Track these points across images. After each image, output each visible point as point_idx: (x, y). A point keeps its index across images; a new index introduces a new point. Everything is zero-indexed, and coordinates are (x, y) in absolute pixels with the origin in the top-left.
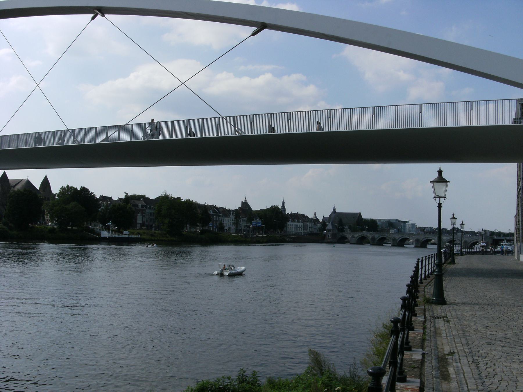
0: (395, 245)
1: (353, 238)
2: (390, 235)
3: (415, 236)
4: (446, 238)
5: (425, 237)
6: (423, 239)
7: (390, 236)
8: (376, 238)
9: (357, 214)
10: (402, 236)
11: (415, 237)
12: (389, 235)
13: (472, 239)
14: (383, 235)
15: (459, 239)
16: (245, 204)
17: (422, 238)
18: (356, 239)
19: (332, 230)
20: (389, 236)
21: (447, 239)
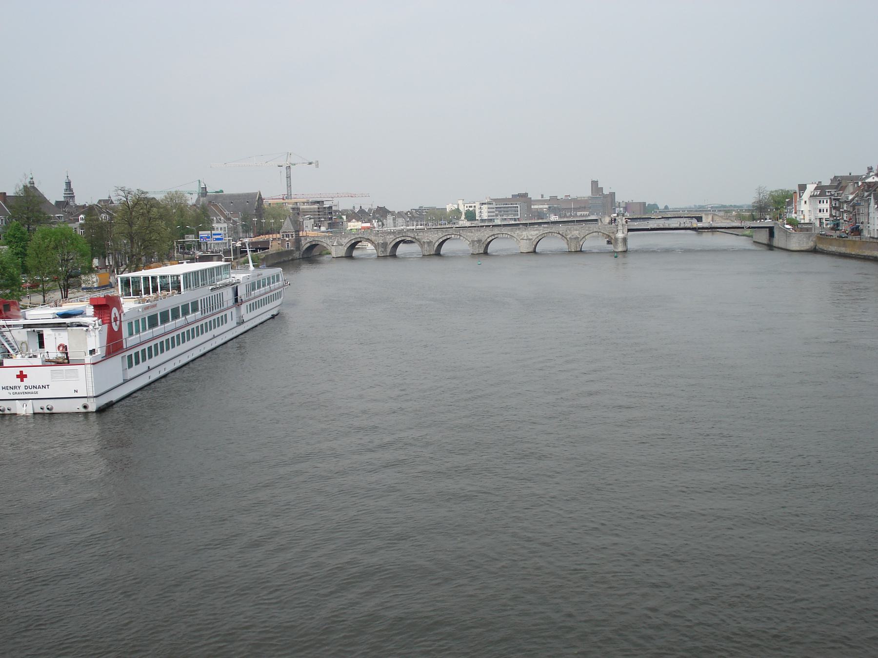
0: (432, 253)
1: (340, 247)
2: (418, 235)
3: (472, 232)
4: (536, 232)
5: (493, 234)
6: (488, 237)
7: (420, 237)
8: (389, 242)
9: (254, 195)
10: (444, 234)
11: (472, 234)
12: (416, 234)
13: (587, 232)
14: (403, 236)
15: (561, 233)
16: (831, 179)
17: (487, 236)
18: (346, 248)
19: (294, 233)
20: (417, 237)
21: (537, 234)
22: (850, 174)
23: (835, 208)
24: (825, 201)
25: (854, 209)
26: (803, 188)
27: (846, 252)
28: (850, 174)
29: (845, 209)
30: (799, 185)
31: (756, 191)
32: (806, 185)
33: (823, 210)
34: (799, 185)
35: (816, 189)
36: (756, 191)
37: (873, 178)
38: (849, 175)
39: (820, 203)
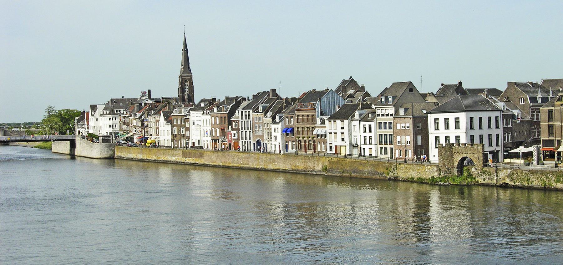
22: (123, 97)
23: (124, 124)
24: (114, 119)
25: (143, 124)
26: (94, 108)
27: (143, 158)
28: (123, 97)
29: (135, 124)
30: (276, 90)
31: (46, 110)
32: (96, 106)
33: (113, 125)
34: (276, 90)
35: (105, 109)
36: (46, 110)
37: (147, 100)
38: (122, 98)
39: (110, 120)
